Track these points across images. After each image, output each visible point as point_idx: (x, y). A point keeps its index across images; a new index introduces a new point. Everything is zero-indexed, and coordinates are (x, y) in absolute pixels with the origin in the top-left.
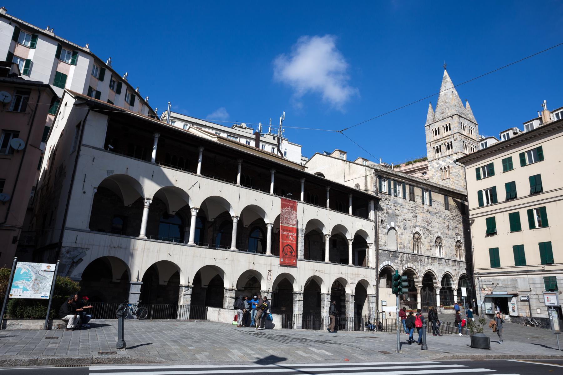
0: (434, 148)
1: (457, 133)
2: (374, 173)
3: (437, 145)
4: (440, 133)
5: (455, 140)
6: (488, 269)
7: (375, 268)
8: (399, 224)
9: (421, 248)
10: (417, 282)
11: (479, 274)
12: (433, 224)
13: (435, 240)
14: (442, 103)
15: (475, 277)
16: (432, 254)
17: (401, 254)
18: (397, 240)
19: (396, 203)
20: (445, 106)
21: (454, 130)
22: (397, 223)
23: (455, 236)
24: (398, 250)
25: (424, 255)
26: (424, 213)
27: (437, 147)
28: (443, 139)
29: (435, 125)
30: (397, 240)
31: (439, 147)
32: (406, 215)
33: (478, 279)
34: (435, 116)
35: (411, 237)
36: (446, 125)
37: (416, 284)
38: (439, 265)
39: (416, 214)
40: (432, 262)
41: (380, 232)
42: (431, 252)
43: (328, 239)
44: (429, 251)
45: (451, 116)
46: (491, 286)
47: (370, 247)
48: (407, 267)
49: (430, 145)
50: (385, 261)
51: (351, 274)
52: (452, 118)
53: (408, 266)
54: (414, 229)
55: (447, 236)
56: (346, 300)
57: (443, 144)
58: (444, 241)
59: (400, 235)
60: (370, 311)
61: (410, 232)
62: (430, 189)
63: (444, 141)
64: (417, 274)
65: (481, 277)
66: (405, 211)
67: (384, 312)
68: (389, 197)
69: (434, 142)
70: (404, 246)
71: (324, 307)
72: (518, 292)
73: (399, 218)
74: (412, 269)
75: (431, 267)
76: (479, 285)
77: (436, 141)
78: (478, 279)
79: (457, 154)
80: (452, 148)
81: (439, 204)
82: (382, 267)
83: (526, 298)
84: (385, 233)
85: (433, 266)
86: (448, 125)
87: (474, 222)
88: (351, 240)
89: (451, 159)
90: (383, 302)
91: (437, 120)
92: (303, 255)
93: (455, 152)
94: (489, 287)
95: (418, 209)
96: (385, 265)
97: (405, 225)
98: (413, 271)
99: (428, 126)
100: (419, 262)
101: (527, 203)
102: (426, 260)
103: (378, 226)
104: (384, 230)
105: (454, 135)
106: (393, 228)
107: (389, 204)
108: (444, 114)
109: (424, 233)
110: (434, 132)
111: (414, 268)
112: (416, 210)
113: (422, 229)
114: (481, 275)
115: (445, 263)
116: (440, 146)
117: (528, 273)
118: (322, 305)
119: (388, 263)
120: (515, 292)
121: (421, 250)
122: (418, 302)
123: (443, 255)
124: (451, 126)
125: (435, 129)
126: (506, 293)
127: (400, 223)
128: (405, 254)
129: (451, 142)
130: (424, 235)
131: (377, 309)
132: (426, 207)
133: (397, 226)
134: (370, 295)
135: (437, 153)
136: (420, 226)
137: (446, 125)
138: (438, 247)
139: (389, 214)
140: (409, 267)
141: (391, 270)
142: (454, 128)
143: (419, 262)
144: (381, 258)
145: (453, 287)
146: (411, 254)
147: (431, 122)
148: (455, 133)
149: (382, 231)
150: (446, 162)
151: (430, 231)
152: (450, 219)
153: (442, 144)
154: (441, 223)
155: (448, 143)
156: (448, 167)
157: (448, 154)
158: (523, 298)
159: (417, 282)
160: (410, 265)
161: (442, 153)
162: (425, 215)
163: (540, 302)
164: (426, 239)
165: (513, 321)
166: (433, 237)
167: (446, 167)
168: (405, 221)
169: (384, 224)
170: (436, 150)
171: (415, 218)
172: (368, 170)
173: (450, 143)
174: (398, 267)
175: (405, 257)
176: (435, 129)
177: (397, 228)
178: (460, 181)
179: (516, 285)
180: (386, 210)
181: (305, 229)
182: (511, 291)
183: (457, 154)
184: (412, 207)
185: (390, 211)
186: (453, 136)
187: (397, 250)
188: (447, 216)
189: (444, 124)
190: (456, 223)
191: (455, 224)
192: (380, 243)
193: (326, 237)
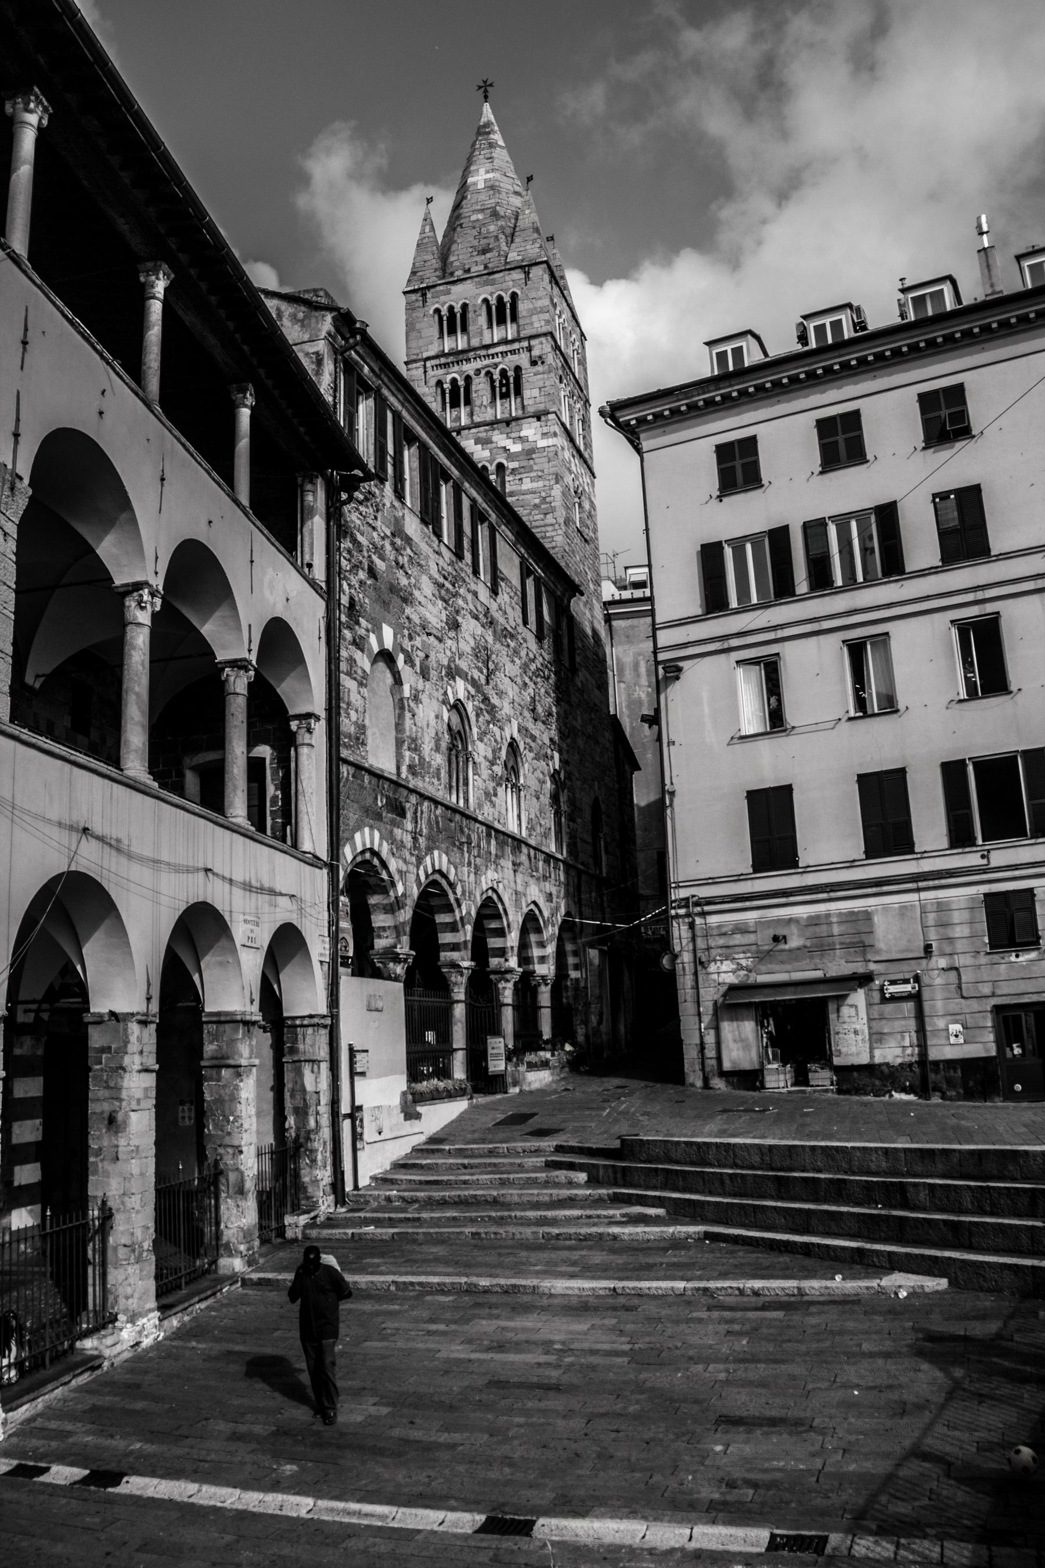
0: (439, 383)
1: (545, 335)
2: (329, 333)
3: (454, 373)
4: (471, 328)
5: (534, 363)
6: (739, 878)
7: (324, 855)
8: (407, 645)
9: (466, 784)
10: (455, 947)
11: (697, 904)
12: (502, 680)
13: (503, 754)
14: (480, 216)
15: (677, 916)
16: (496, 816)
17: (413, 799)
18: (397, 725)
19: (398, 531)
20: (492, 228)
21: (532, 324)
22: (403, 636)
23: (549, 751)
24: (404, 776)
25: (480, 818)
26: (476, 618)
27: (454, 381)
28: (483, 352)
29: (448, 292)
30: (399, 726)
31: (461, 383)
32: (430, 606)
33: (692, 926)
34: (452, 259)
35: (442, 719)
36: (500, 299)
37: (445, 956)
38: (515, 871)
39: (457, 612)
40: (499, 853)
41: (343, 666)
42: (494, 806)
43: (144, 617)
44: (491, 801)
45: (521, 267)
46: (749, 951)
47: (303, 737)
48: (430, 871)
49: (421, 370)
50: (359, 828)
51: (244, 884)
52: (527, 274)
53: (433, 865)
54: (451, 682)
55: (533, 744)
56: (205, 1055)
57: (483, 372)
58: (526, 765)
59: (412, 704)
60: (306, 1114)
61: (441, 698)
62: (493, 517)
63: (487, 362)
64: (459, 906)
65: (703, 914)
66: (427, 588)
67: (360, 1108)
68: (377, 491)
69: (443, 360)
70: (422, 758)
71: (120, 1117)
72: (872, 967)
73: (408, 611)
74: (444, 883)
75: (496, 876)
76: (695, 950)
77: (451, 359)
78: (692, 926)
79: (539, 419)
80: (518, 392)
81: (512, 594)
82: (349, 857)
83: (908, 988)
84: (359, 672)
85: (501, 875)
86: (507, 299)
87: (678, 678)
88: (239, 665)
89: (513, 435)
90: (359, 1057)
91: (459, 273)
92: (7, 689)
93: (531, 410)
94: (742, 955)
95: (462, 591)
96: (360, 849)
97: (427, 657)
98: (445, 894)
99: (419, 294)
100: (465, 849)
101: (928, 598)
102: (483, 844)
103: (340, 631)
104: (358, 655)
105: (533, 342)
106: (386, 657)
107: (378, 524)
108: (488, 255)
109: (478, 716)
110: (445, 318)
111: (452, 877)
112: (456, 595)
113: (473, 691)
114: (707, 908)
115: (526, 862)
116: (468, 379)
117: (921, 884)
118: (93, 1107)
119: (372, 842)
120: (860, 968)
121: (466, 793)
122: (455, 1046)
123: (520, 825)
124: (523, 307)
125: (451, 309)
126: (819, 974)
127: (411, 638)
128: (426, 804)
129: (518, 369)
130: (477, 721)
131: (335, 1103)
132: (484, 594)
133: (403, 650)
134: (306, 1022)
135: (451, 407)
136: (467, 674)
137: (500, 299)
138: (509, 790)
139: (376, 579)
140: (437, 868)
141: (372, 881)
142: (534, 312)
143: (465, 849)
144: (350, 814)
145: (541, 969)
146: (443, 805)
147: (433, 280)
148: (534, 332)
149: (351, 657)
150: (489, 446)
151: (494, 707)
152: (537, 673)
153: (478, 372)
154: (519, 680)
155: (503, 372)
156: (500, 467)
157: (499, 417)
158: (893, 989)
159: (455, 947)
160: (439, 859)
161: (477, 409)
162: (479, 630)
163: (963, 997)
164: (482, 741)
165: (845, 1087)
166: (499, 739)
167: (492, 468)
168: (425, 637)
169: (358, 623)
170: (447, 395)
171: (452, 634)
172: (294, 317)
173: (511, 374)
174: (404, 869)
175: (425, 815)
176: (451, 309)
177: (400, 659)
178: (550, 528)
179: (864, 937)
180: (366, 554)
181: (26, 481)
182: (839, 966)
183: (543, 418)
184: (445, 578)
185: (380, 565)
186: (525, 344)
187: (399, 774)
188: (531, 656)
189: (491, 294)
190: (549, 695)
191: (550, 700)
192: (347, 725)
193: (131, 603)
